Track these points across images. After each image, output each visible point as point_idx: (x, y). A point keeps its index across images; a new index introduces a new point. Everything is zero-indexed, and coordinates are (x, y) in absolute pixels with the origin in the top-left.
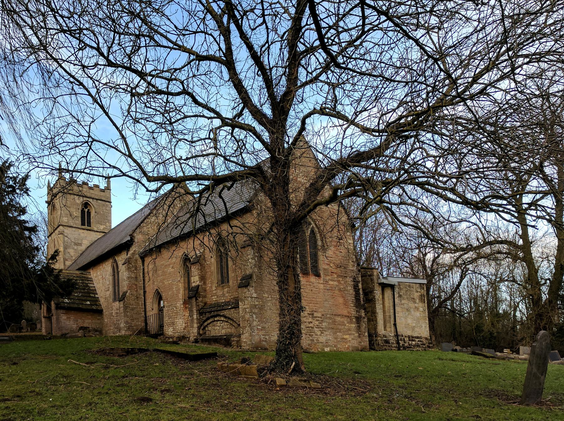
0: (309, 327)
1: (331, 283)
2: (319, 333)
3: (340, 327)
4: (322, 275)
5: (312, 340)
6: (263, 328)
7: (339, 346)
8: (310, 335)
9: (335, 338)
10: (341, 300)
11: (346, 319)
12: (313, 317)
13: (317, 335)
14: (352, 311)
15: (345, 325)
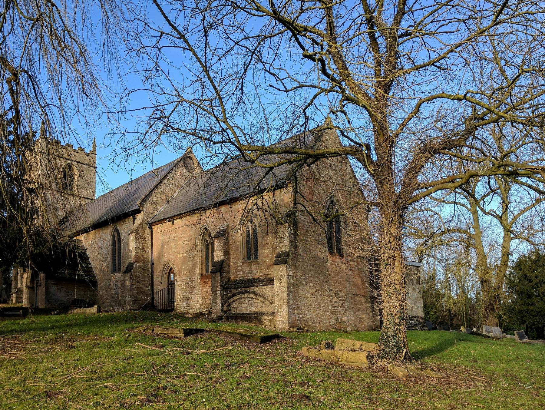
1: (352, 263)
2: (342, 312)
5: (338, 320)
8: (335, 314)
9: (355, 318)
12: (339, 297)
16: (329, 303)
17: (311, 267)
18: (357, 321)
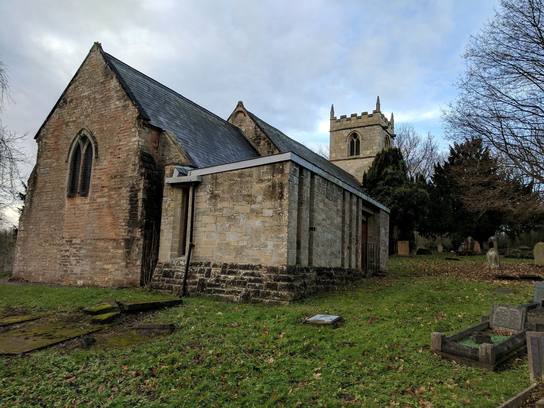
0: (65, 256)
2: (74, 263)
6: (24, 258)
7: (95, 279)
8: (64, 265)
9: (93, 269)
10: (109, 219)
11: (111, 243)
13: (72, 265)
15: (109, 251)
17: (43, 218)
18: (95, 273)
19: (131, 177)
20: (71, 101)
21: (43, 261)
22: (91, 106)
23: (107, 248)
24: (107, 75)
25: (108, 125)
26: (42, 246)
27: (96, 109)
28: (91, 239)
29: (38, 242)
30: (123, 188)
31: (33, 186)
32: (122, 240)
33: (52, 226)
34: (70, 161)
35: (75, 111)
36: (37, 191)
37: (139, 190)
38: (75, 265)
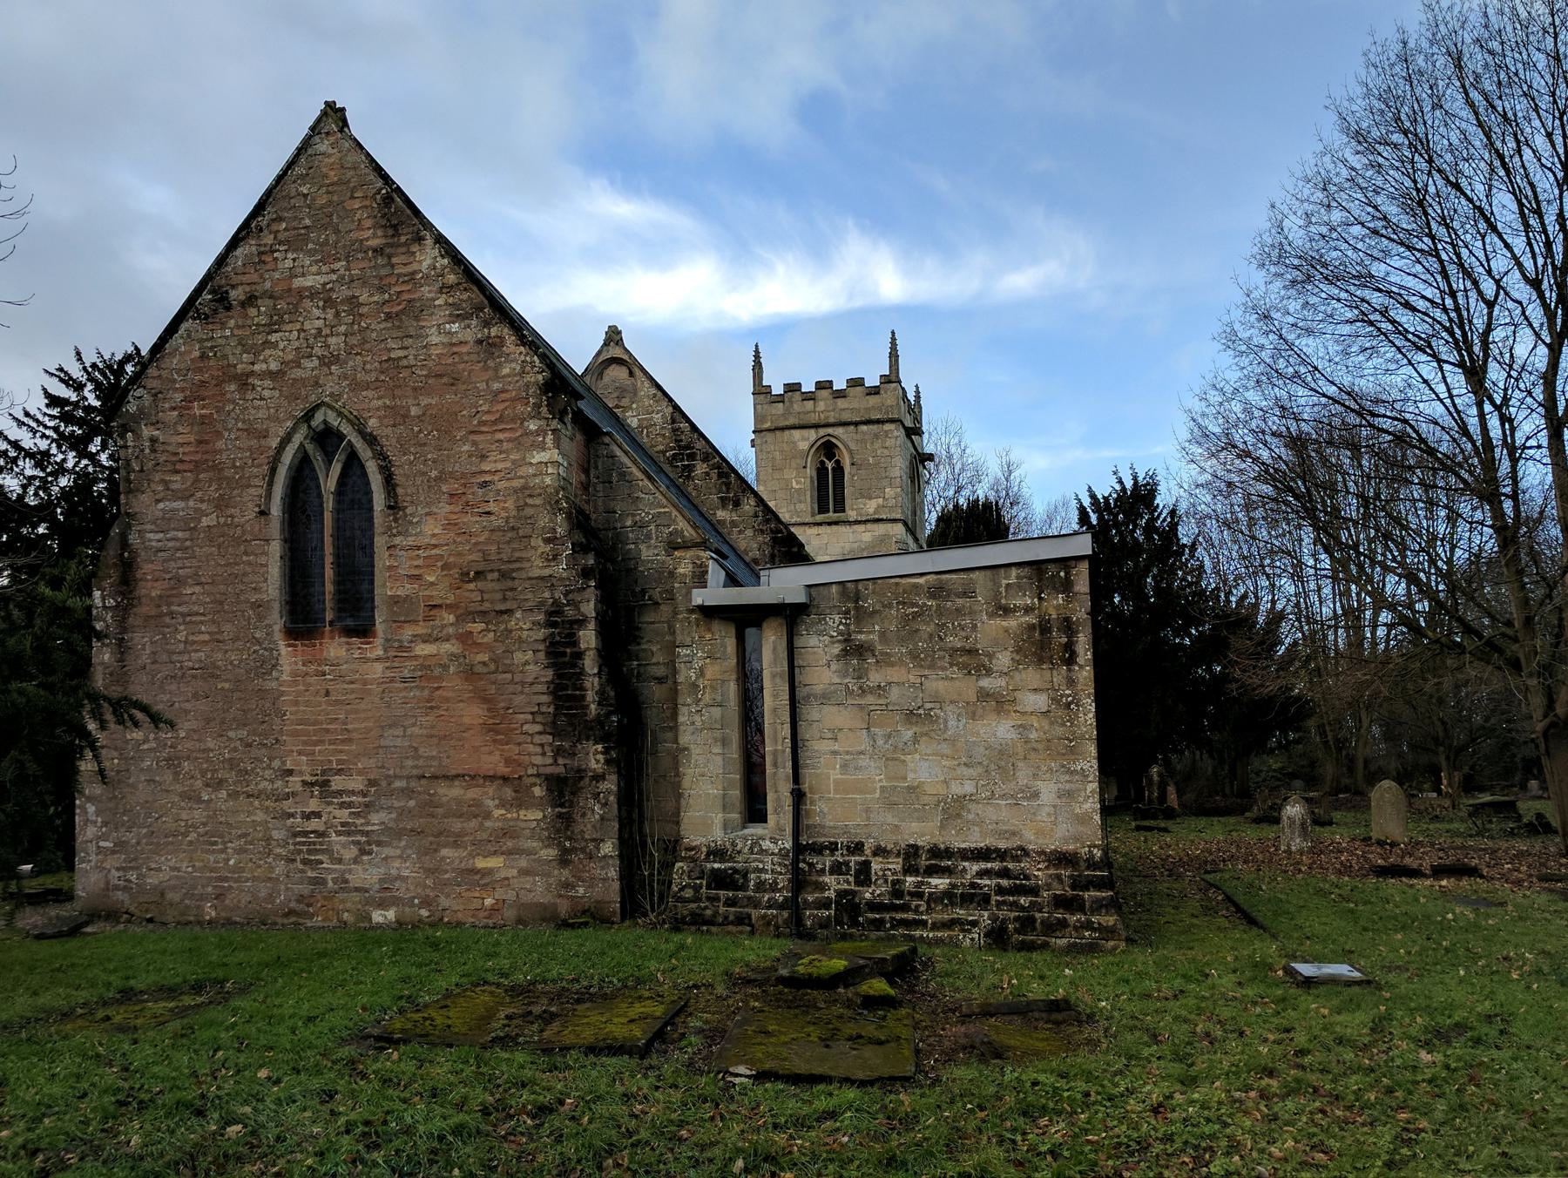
0: (305, 834)
3: (457, 825)
4: (380, 627)
6: (120, 846)
7: (444, 902)
9: (430, 872)
10: (473, 714)
11: (491, 790)
13: (340, 861)
14: (537, 755)
15: (488, 816)
16: (273, 823)
17: (188, 706)
19: (542, 578)
20: (251, 300)
21: (214, 852)
22: (343, 329)
23: (477, 803)
24: (395, 227)
25: (425, 401)
26: (199, 800)
27: (364, 341)
28: (408, 778)
29: (179, 788)
30: (518, 615)
31: (122, 593)
32: (533, 780)
33: (231, 734)
34: (276, 510)
35: (273, 338)
36: (144, 610)
37: (581, 622)
38: (356, 861)
